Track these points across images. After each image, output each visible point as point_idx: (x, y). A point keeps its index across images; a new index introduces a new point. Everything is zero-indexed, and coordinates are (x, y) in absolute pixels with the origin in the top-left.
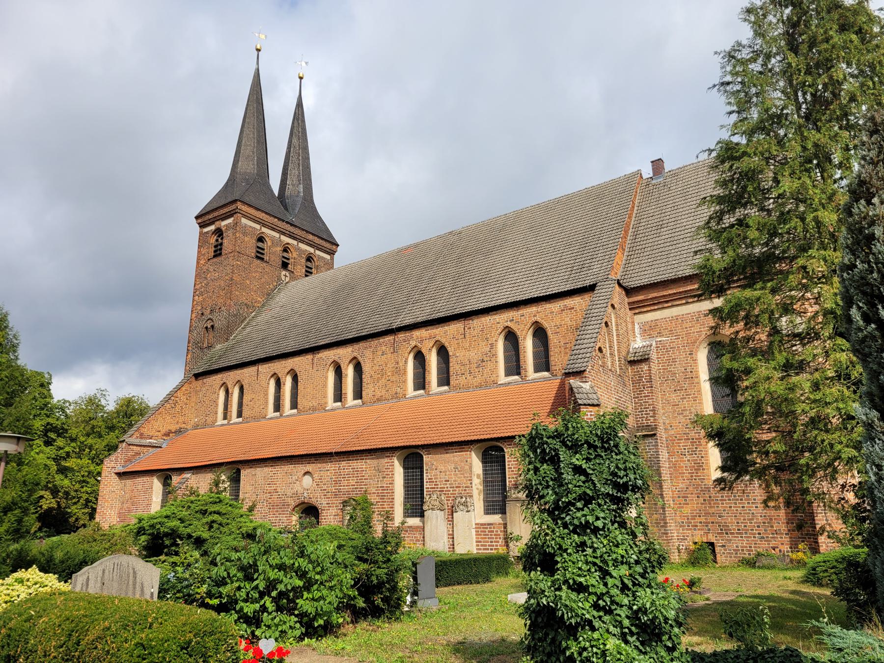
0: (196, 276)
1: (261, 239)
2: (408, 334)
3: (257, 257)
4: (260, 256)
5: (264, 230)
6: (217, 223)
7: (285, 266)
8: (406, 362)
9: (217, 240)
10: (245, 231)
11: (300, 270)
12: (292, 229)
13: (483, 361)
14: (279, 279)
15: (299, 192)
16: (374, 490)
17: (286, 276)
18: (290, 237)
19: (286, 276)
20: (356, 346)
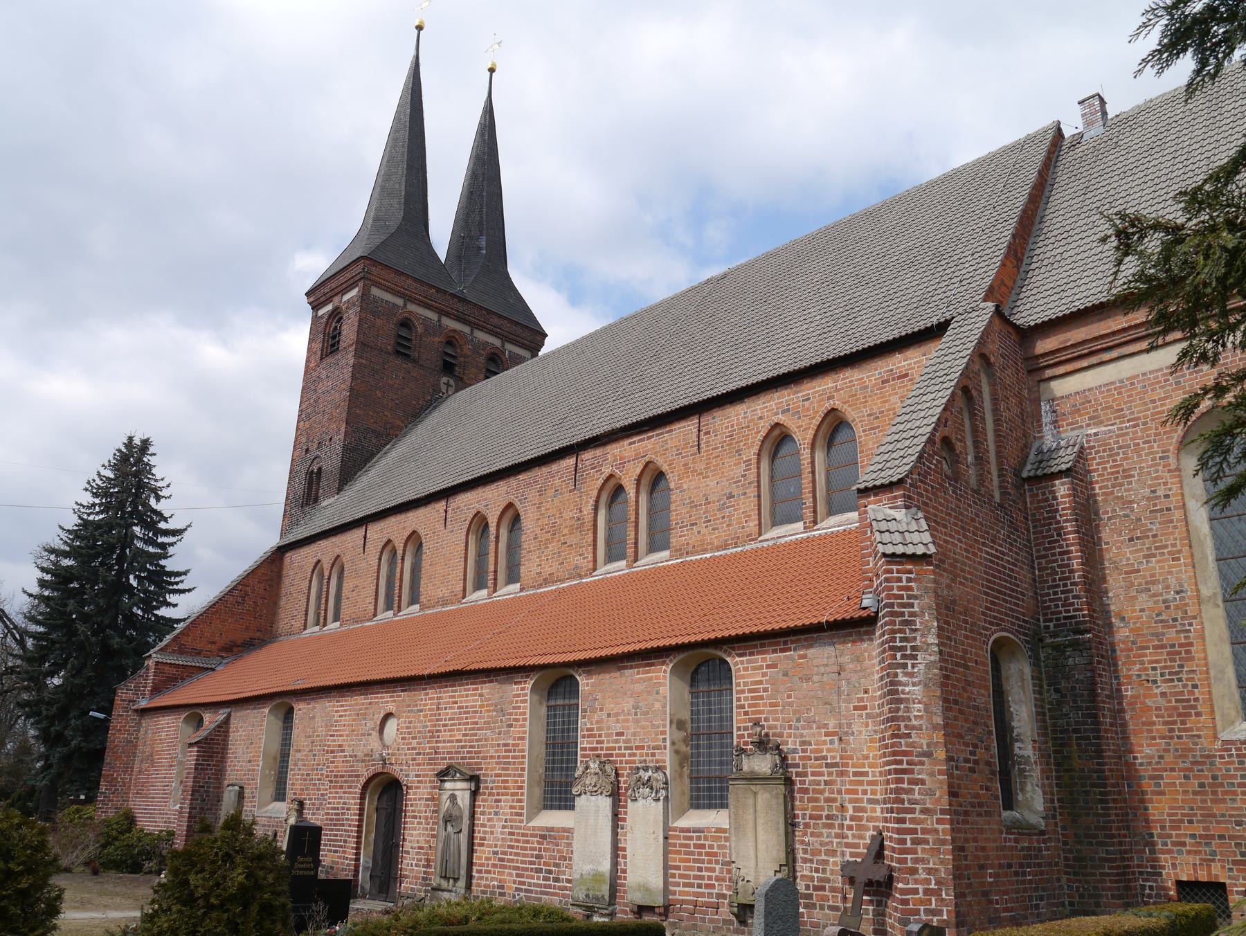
0: (303, 388)
1: (406, 324)
2: (599, 452)
3: (398, 353)
4: (402, 349)
8: (596, 509)
12: (460, 307)
13: (731, 496)
16: (492, 752)
17: (448, 385)
18: (458, 319)
19: (448, 385)
20: (513, 482)
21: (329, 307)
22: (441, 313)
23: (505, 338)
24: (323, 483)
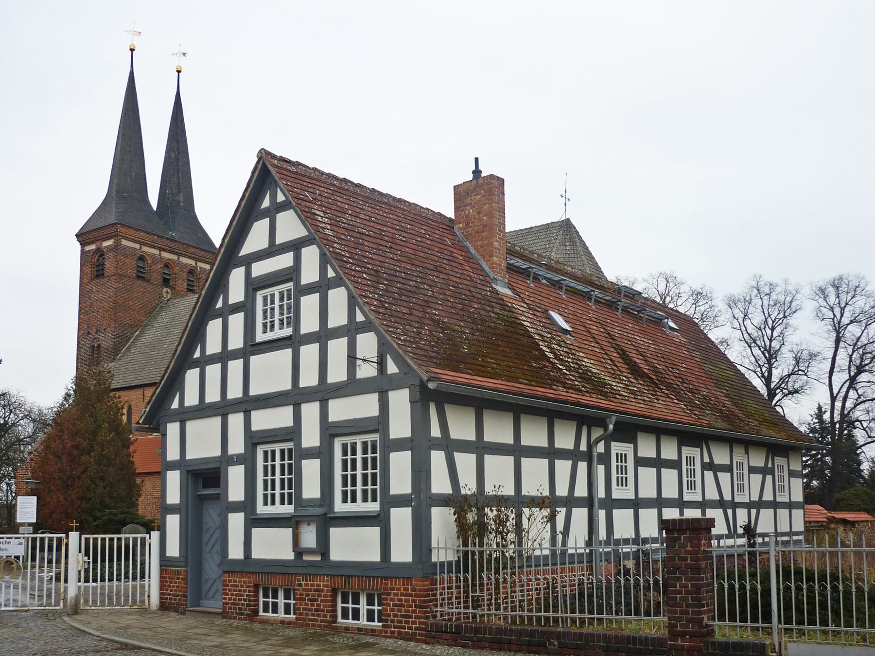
1: (142, 258)
4: (141, 276)
5: (145, 249)
6: (98, 243)
7: (166, 282)
9: (98, 260)
11: (182, 285)
12: (172, 244)
14: (161, 296)
15: (179, 202)
17: (167, 292)
19: (167, 292)
21: (93, 247)
22: (161, 249)
23: (197, 260)
24: (103, 354)
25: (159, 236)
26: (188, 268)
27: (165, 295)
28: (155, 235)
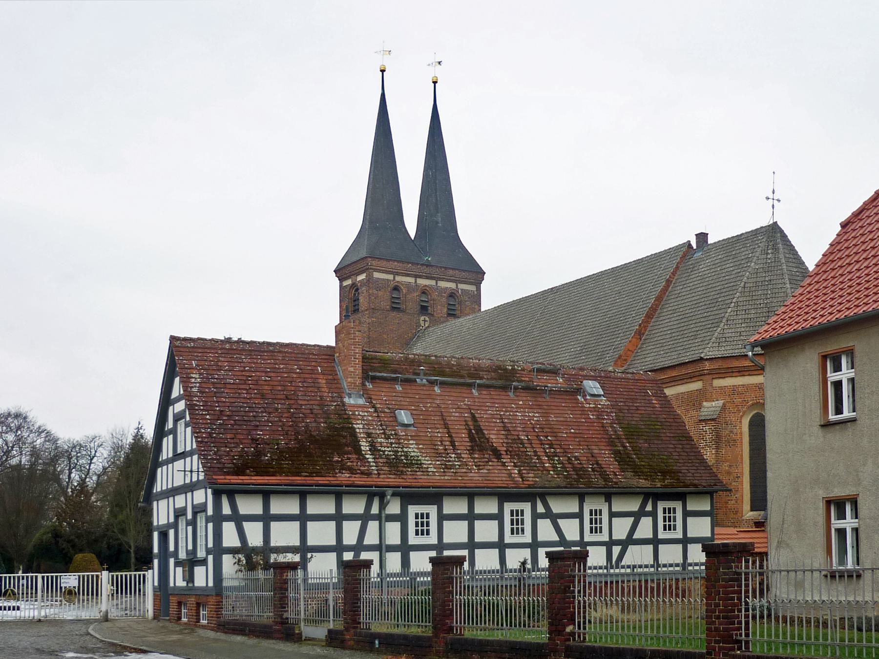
3: (394, 309)
5: (398, 278)
7: (424, 309)
10: (380, 285)
11: (441, 310)
15: (437, 223)
17: (425, 321)
18: (427, 278)
19: (425, 321)
22: (416, 277)
25: (413, 264)
26: (448, 292)
27: (422, 323)
28: (408, 263)
